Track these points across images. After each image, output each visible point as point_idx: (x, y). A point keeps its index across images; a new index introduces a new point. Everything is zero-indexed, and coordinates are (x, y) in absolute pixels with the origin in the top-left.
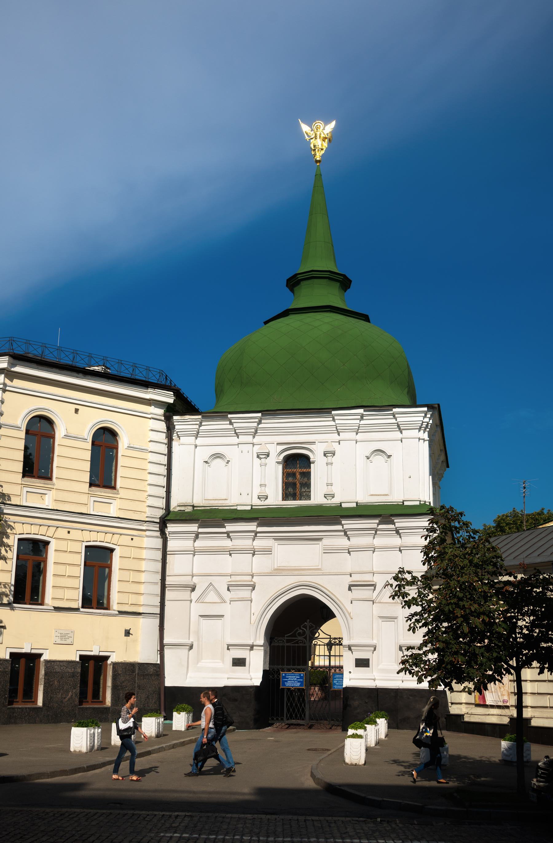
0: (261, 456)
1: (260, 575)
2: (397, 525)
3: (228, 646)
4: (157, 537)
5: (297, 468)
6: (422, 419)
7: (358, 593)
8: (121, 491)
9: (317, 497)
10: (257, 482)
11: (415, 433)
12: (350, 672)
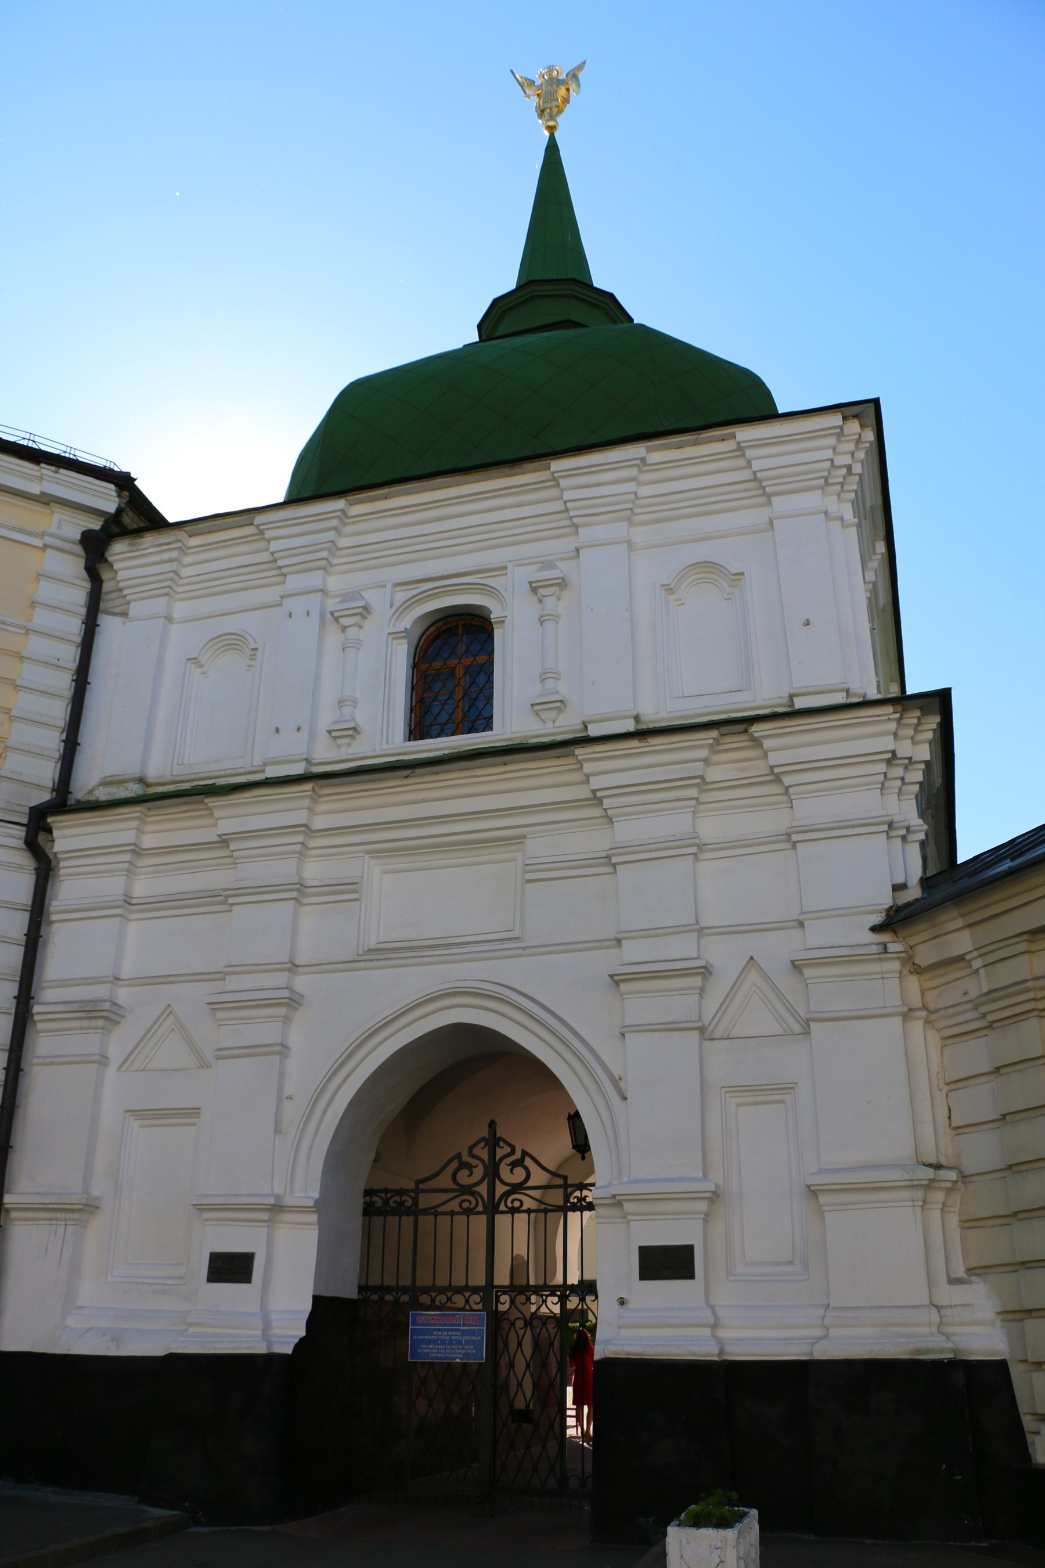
0: (344, 621)
1: (318, 967)
4: (21, 867)
6: (829, 453)
7: (643, 1005)
9: (512, 719)
10: (328, 697)
11: (813, 500)
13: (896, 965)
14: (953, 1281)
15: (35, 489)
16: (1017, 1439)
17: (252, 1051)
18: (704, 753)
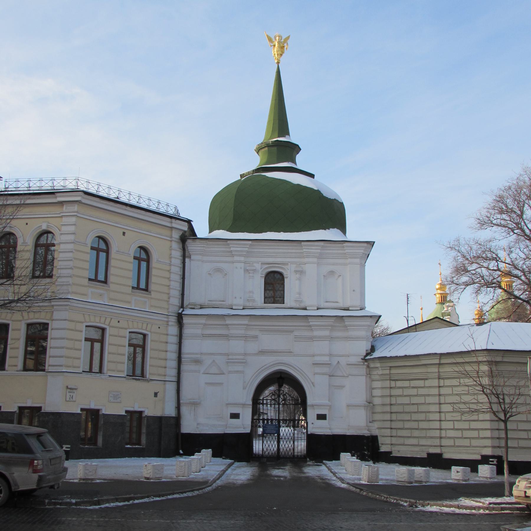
2: (347, 323)
3: (227, 404)
8: (152, 293)
12: (313, 423)
13: (365, 367)
14: (370, 422)
15: (169, 225)
16: (378, 448)
17: (237, 372)
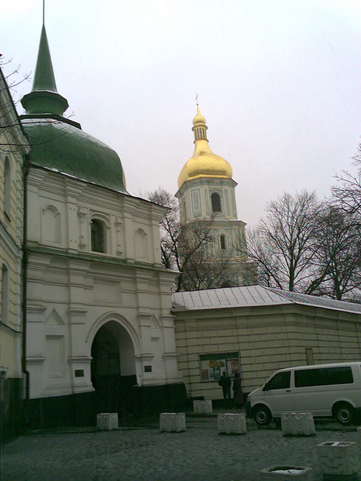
2: (161, 278)
5: (98, 229)
9: (111, 252)
18: (152, 274)
